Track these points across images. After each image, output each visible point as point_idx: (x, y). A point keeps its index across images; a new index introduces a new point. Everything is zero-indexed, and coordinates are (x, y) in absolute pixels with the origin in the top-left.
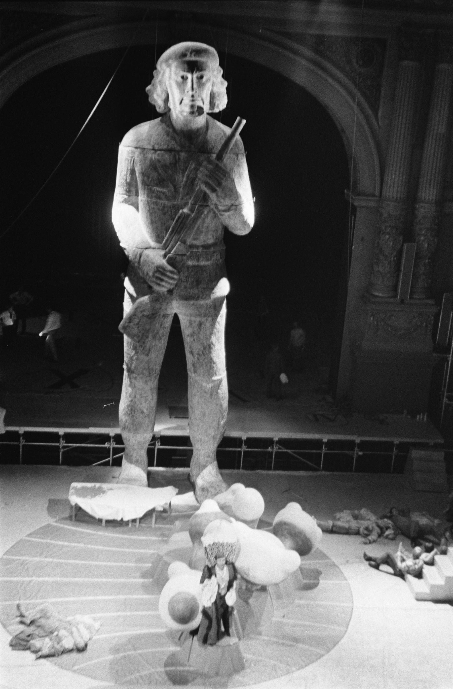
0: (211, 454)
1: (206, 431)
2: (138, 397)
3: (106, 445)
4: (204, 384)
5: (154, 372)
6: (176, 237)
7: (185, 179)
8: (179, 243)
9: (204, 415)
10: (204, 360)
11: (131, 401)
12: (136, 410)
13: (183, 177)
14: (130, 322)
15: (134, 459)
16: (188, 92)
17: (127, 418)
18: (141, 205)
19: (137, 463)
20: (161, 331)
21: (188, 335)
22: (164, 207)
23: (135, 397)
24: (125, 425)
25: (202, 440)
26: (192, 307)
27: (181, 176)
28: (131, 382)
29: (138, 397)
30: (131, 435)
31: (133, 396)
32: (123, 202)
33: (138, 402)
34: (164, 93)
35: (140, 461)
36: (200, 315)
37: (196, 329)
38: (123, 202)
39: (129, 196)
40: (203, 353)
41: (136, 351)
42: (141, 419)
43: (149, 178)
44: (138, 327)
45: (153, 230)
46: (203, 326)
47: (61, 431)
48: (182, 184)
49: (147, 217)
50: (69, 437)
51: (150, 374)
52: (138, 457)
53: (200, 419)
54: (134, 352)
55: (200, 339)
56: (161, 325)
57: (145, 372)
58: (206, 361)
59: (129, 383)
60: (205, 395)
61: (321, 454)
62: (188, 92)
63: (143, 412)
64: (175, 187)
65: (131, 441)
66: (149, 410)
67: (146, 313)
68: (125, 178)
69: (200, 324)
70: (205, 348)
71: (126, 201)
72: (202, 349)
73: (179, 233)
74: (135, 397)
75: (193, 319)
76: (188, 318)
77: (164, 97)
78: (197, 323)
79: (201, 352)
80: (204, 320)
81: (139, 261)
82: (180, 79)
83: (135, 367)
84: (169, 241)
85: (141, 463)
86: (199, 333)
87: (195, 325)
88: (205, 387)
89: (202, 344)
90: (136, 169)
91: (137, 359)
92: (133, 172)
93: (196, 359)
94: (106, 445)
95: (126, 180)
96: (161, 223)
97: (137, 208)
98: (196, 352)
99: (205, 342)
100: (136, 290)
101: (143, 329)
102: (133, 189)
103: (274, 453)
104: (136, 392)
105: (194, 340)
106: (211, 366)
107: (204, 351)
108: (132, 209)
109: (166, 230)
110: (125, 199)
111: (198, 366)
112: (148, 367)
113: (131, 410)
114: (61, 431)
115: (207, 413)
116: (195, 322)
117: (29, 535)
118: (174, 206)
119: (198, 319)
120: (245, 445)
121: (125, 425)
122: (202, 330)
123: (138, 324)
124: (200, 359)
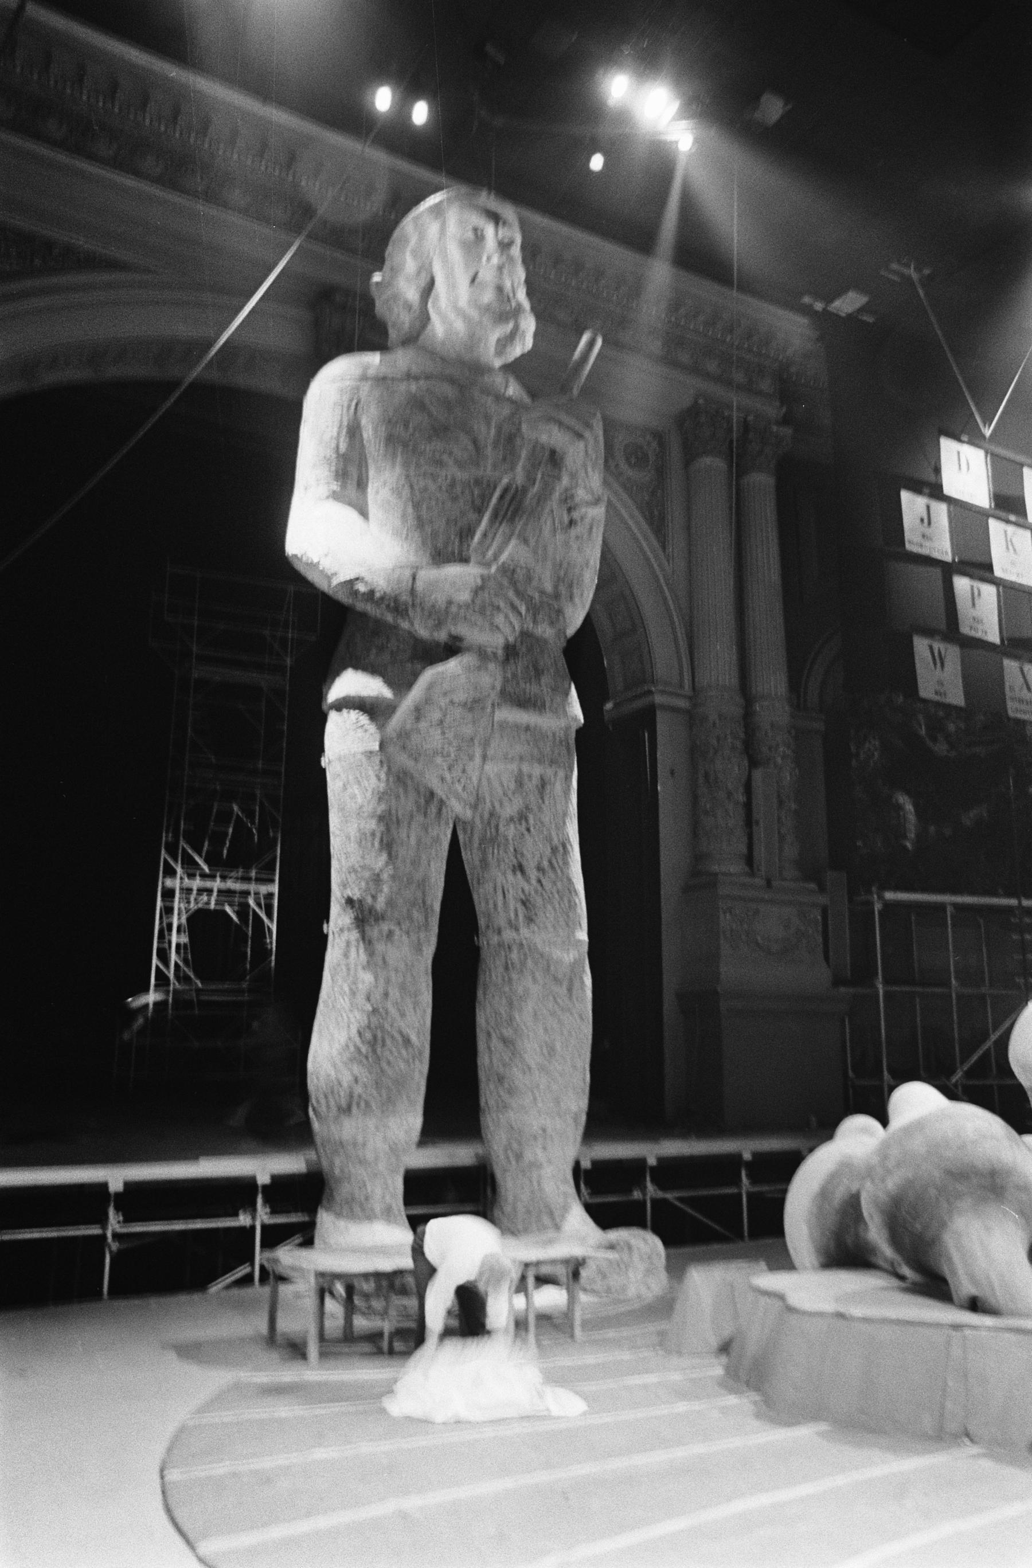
1: (557, 1101)
2: (395, 993)
3: (243, 1220)
4: (557, 953)
6: (504, 528)
7: (493, 431)
8: (513, 542)
9: (552, 1050)
10: (554, 883)
11: (375, 1011)
12: (388, 1042)
13: (489, 428)
14: (418, 719)
15: (378, 1208)
16: (489, 259)
17: (356, 1069)
18: (373, 509)
19: (388, 1214)
21: (512, 819)
22: (453, 484)
23: (386, 995)
24: (351, 1096)
25: (549, 1131)
27: (483, 428)
28: (371, 953)
29: (395, 993)
30: (371, 1123)
31: (377, 996)
32: (328, 497)
33: (393, 1011)
34: (423, 275)
36: (540, 761)
38: (328, 497)
39: (344, 486)
40: (550, 862)
41: (390, 855)
43: (406, 426)
44: (443, 733)
45: (424, 543)
47: (115, 1177)
48: (490, 441)
49: (404, 516)
50: (139, 1199)
53: (542, 1068)
54: (384, 857)
59: (363, 957)
60: (556, 989)
61: (740, 1195)
62: (489, 259)
63: (407, 1041)
64: (475, 442)
65: (370, 1145)
67: (460, 696)
68: (333, 445)
69: (543, 784)
70: (554, 850)
71: (335, 496)
73: (512, 520)
74: (386, 995)
75: (526, 768)
76: (514, 767)
77: (423, 282)
78: (535, 781)
79: (545, 864)
80: (549, 772)
81: (413, 591)
82: (470, 235)
83: (390, 903)
84: (490, 535)
86: (540, 808)
87: (531, 785)
88: (559, 962)
89: (549, 839)
90: (364, 421)
91: (393, 877)
92: (353, 431)
93: (534, 882)
94: (243, 1220)
95: (338, 447)
96: (448, 522)
97: (364, 513)
99: (554, 834)
100: (389, 682)
101: (456, 736)
102: (353, 471)
103: (649, 1205)
104: (388, 981)
106: (569, 901)
107: (554, 861)
108: (352, 514)
109: (461, 537)
110: (334, 492)
111: (539, 901)
113: (373, 1043)
114: (115, 1177)
115: (558, 1046)
117: (201, 1410)
118: (478, 482)
119: (537, 770)
121: (351, 1096)
123: (441, 722)
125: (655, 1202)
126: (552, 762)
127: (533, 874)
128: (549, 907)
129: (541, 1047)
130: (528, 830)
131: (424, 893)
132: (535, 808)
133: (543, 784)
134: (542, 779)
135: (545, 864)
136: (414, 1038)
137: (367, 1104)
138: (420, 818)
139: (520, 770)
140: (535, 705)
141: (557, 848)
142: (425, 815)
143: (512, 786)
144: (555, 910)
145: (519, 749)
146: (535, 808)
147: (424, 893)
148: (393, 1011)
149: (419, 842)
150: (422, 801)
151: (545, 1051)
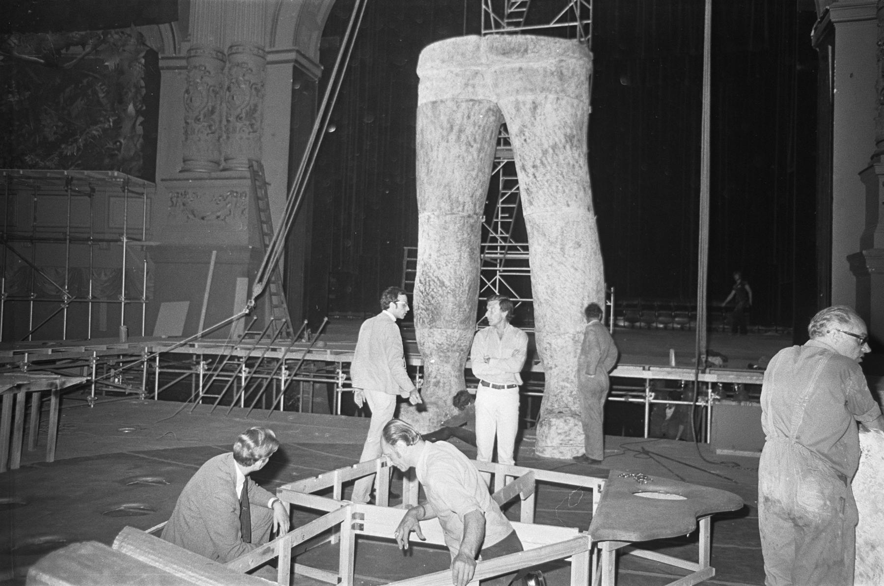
0: (572, 377)
5: (460, 208)
20: (469, 130)
25: (553, 346)
26: (518, 76)
33: (434, 266)
35: (441, 385)
37: (527, 118)
40: (542, 163)
42: (439, 298)
46: (538, 111)
51: (452, 209)
52: (438, 377)
55: (535, 135)
56: (469, 117)
57: (443, 205)
58: (548, 176)
60: (552, 249)
63: (443, 284)
66: (453, 281)
69: (535, 106)
72: (540, 155)
75: (520, 98)
76: (512, 99)
78: (528, 106)
79: (538, 163)
80: (540, 98)
85: (444, 387)
86: (533, 124)
87: (526, 109)
89: (541, 144)
93: (532, 177)
98: (529, 165)
99: (544, 140)
105: (525, 140)
107: (544, 159)
111: (534, 190)
112: (450, 197)
116: (524, 105)
119: (530, 97)
120: (651, 390)
122: (538, 118)
124: (537, 175)
125: (652, 405)
126: (543, 90)
127: (531, 171)
128: (541, 192)
129: (546, 288)
130: (525, 140)
131: (449, 191)
132: (529, 125)
133: (535, 106)
134: (534, 103)
135: (538, 163)
136: (447, 283)
137: (424, 322)
138: (444, 144)
139: (517, 100)
140: (518, 51)
141: (546, 150)
142: (447, 142)
143: (514, 111)
144: (544, 193)
145: (517, 84)
146: (529, 125)
147: (449, 191)
148: (434, 266)
149: (445, 159)
150: (445, 133)
151: (549, 292)
